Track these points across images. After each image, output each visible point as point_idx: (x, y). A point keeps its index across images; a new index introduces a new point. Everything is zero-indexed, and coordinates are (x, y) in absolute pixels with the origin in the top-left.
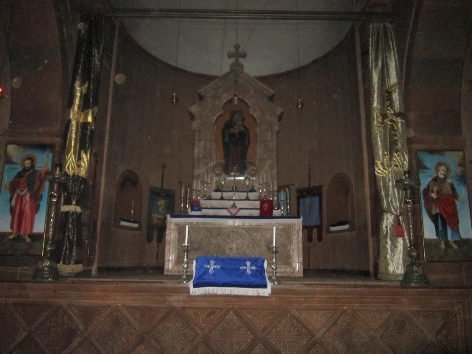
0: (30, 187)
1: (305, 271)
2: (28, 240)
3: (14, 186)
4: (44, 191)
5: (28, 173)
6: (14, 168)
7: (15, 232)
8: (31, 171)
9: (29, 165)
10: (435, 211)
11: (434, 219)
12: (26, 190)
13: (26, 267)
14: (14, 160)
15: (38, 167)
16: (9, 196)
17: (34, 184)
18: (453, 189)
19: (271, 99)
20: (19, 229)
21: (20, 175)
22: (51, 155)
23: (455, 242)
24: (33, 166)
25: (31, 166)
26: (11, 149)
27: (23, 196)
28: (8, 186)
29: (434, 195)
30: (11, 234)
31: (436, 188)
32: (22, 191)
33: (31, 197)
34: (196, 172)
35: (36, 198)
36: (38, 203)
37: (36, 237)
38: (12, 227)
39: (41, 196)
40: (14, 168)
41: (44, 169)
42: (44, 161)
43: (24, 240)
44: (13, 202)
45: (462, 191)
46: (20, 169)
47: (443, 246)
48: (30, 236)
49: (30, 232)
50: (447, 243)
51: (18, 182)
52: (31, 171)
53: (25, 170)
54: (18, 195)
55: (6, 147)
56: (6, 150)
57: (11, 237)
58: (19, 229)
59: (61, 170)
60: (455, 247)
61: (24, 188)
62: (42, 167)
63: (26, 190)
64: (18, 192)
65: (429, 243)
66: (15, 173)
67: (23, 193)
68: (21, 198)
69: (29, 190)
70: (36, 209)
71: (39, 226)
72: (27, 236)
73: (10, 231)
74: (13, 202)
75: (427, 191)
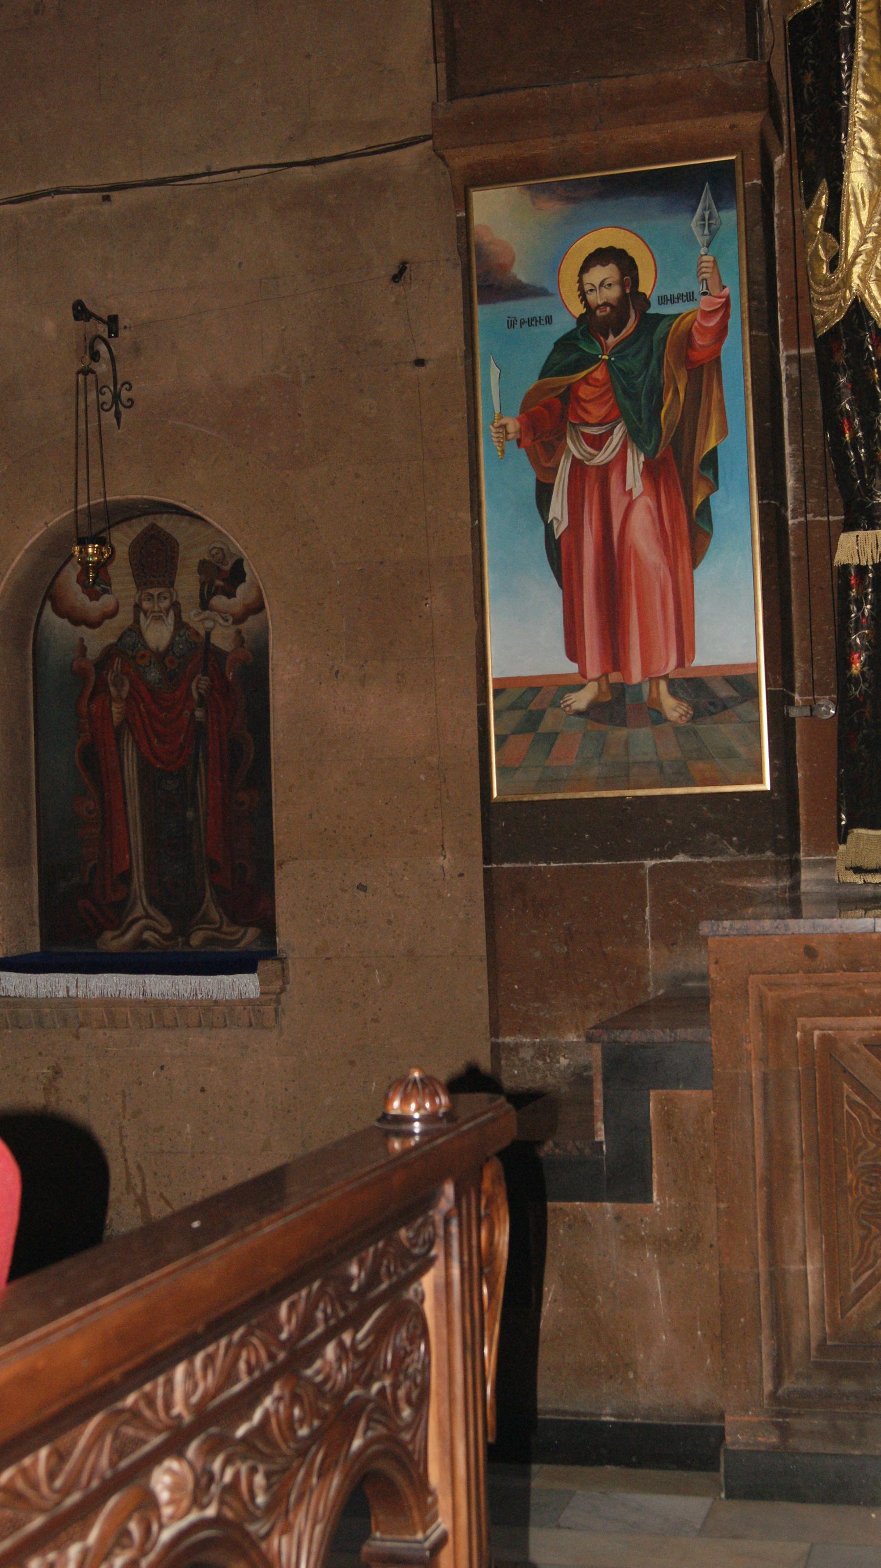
2: (673, 708)
3: (545, 424)
4: (724, 431)
5: (612, 340)
6: (532, 322)
7: (593, 671)
8: (631, 324)
9: (613, 294)
12: (619, 432)
13: (681, 858)
14: (521, 273)
15: (663, 300)
16: (529, 479)
17: (656, 395)
20: (615, 656)
21: (569, 354)
22: (729, 219)
24: (632, 296)
25: (624, 299)
26: (496, 211)
27: (604, 471)
28: (513, 427)
30: (568, 686)
32: (598, 442)
33: (651, 472)
35: (681, 472)
36: (698, 500)
37: (714, 696)
38: (574, 650)
39: (711, 460)
40: (532, 322)
41: (703, 304)
42: (690, 263)
43: (658, 717)
44: (558, 508)
46: (564, 324)
48: (675, 687)
49: (681, 663)
51: (569, 395)
52: (631, 324)
53: (590, 324)
54: (578, 468)
55: (466, 205)
56: (465, 225)
57: (581, 700)
58: (615, 656)
59: (850, 292)
61: (607, 421)
62: (690, 297)
63: (619, 432)
64: (574, 448)
67: (602, 457)
69: (635, 436)
70: (691, 535)
71: (730, 626)
72: (663, 686)
73: (572, 668)
74: (558, 508)
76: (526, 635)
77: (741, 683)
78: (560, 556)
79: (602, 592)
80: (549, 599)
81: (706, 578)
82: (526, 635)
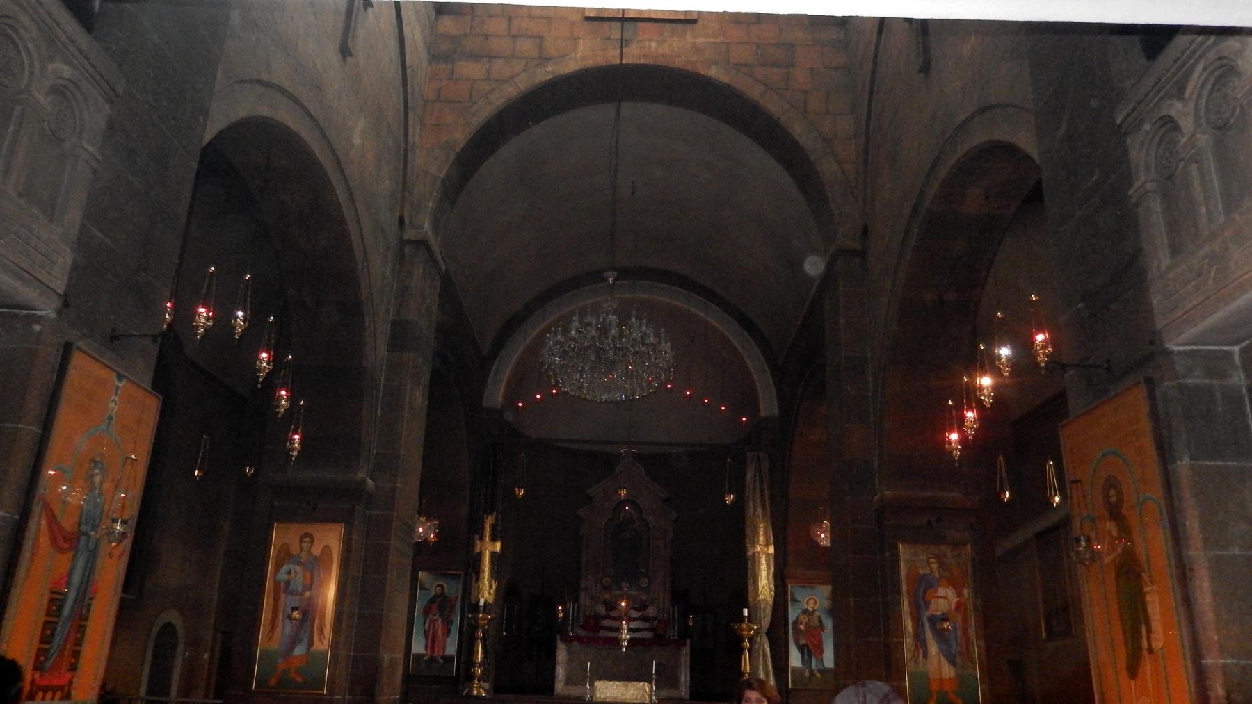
0: (441, 609)
1: (691, 695)
3: (426, 612)
10: (802, 642)
11: (801, 649)
18: (820, 621)
19: (665, 501)
20: (433, 651)
21: (432, 601)
23: (819, 671)
24: (443, 593)
26: (422, 575)
29: (802, 627)
30: (423, 655)
31: (804, 619)
34: (583, 586)
35: (448, 623)
37: (448, 659)
42: (453, 589)
43: (437, 662)
45: (828, 624)
47: (807, 674)
50: (811, 672)
53: (436, 596)
58: (433, 651)
60: (818, 675)
65: (794, 670)
66: (429, 598)
68: (433, 622)
71: (451, 649)
75: (796, 623)
76: (418, 647)
77: (451, 658)
78: (426, 633)
79: (432, 640)
80: (423, 641)
81: (449, 640)
82: (418, 647)
